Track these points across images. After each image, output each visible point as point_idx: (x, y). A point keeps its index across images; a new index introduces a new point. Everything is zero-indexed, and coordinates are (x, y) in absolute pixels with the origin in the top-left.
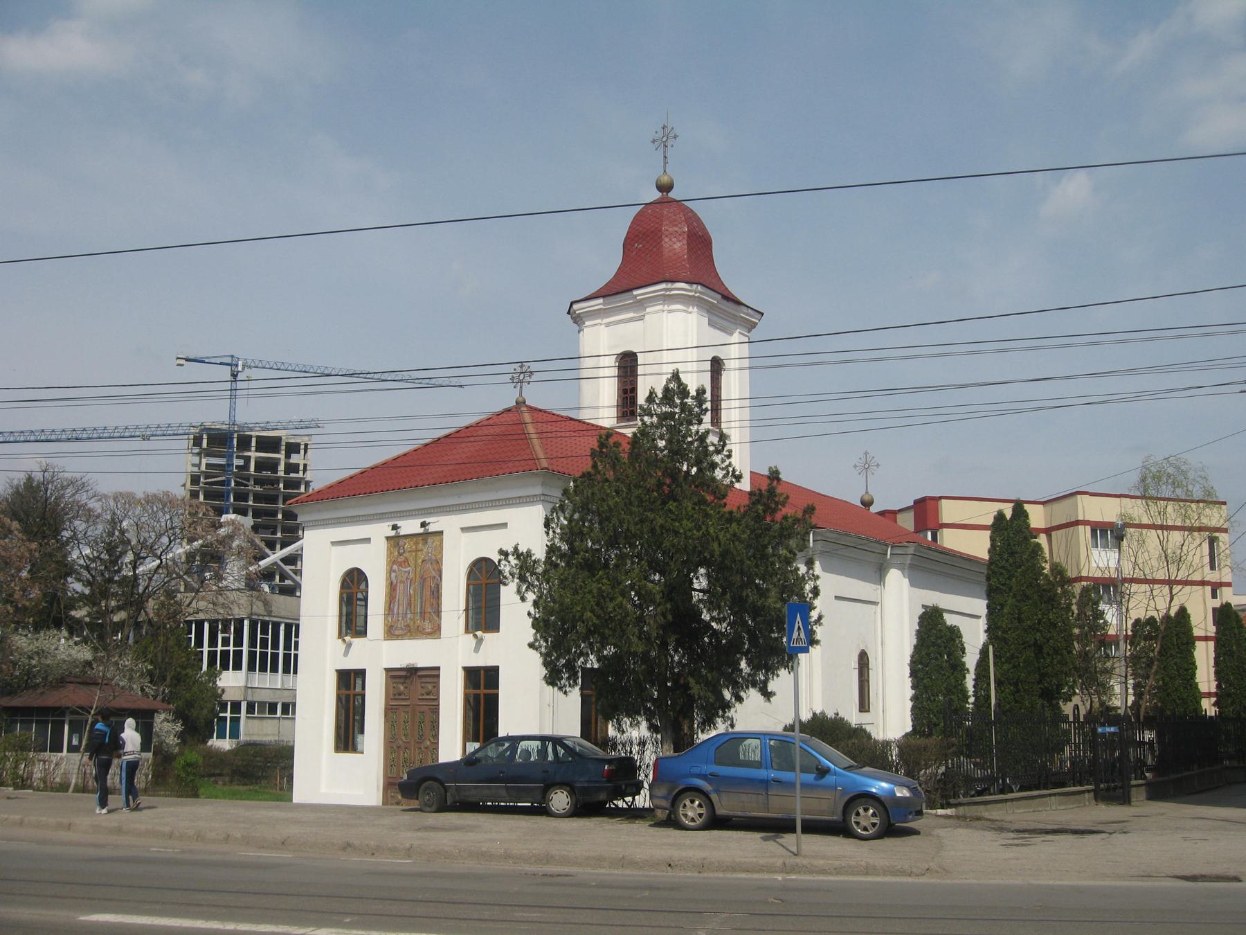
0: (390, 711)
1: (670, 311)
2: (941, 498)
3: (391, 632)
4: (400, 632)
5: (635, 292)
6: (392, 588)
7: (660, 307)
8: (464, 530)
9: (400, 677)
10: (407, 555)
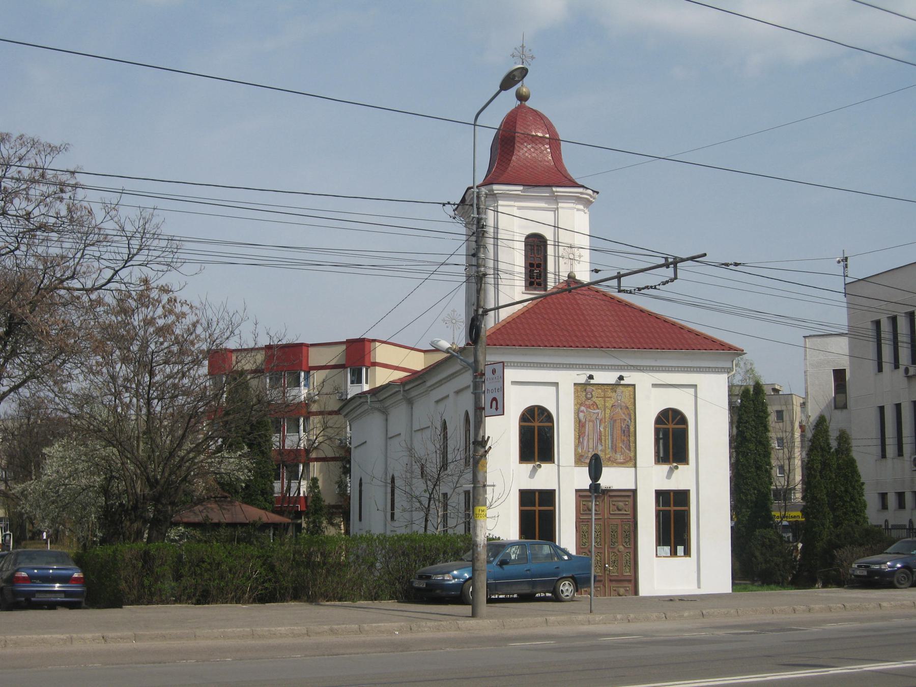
1: (578, 210)
2: (374, 341)
5: (554, 189)
6: (580, 426)
7: (571, 205)
8: (654, 385)
10: (594, 399)
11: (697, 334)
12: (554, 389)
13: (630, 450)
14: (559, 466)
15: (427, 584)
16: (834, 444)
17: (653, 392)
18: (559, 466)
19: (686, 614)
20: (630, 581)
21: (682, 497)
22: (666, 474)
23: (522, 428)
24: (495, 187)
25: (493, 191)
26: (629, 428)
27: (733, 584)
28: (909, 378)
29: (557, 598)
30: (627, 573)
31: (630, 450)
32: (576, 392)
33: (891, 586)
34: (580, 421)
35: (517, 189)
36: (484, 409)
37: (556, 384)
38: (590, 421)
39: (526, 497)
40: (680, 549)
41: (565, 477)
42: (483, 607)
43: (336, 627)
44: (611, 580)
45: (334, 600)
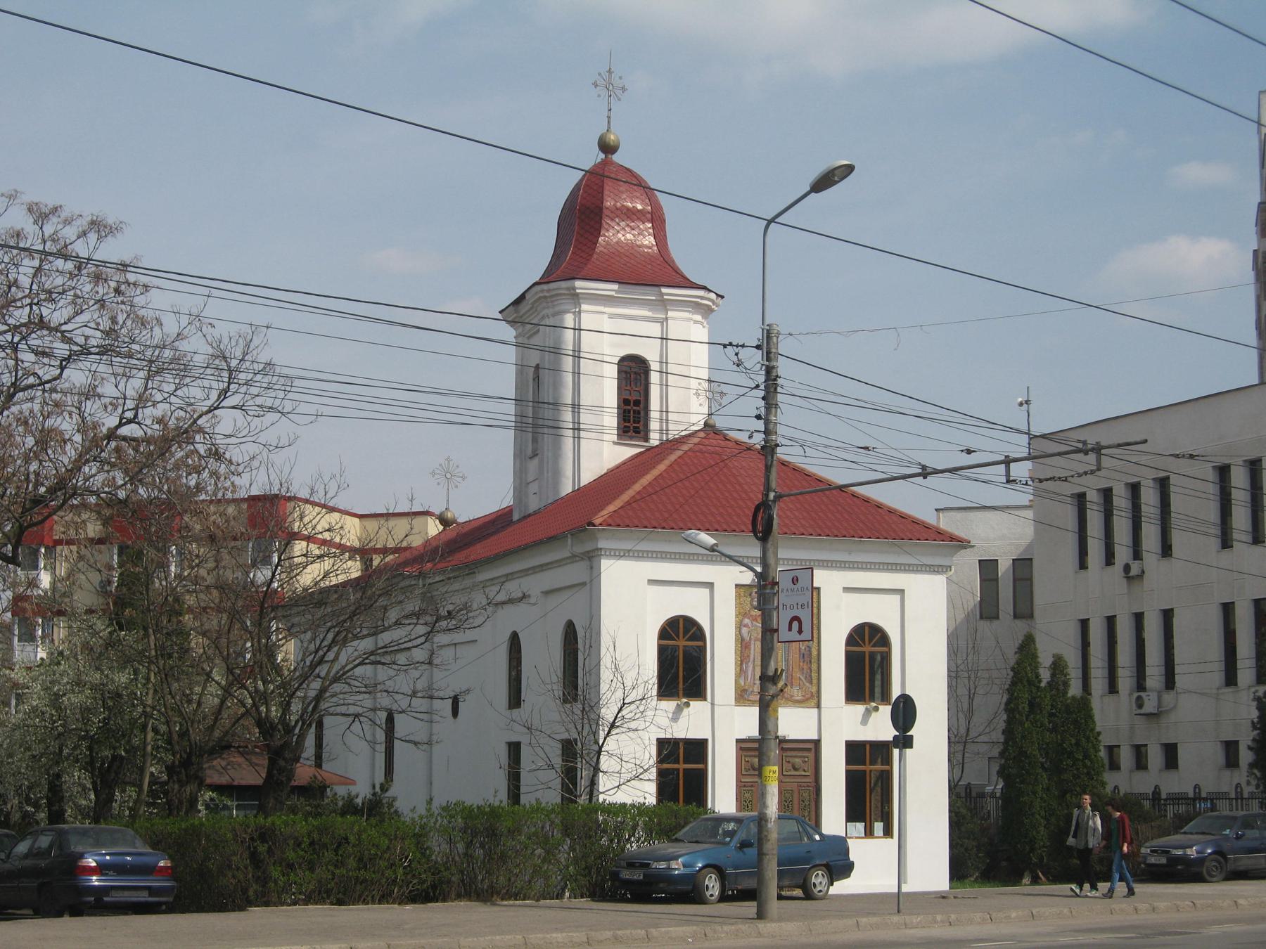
1: (696, 322)
5: (664, 290)
8: (846, 590)
11: (903, 517)
12: (705, 592)
14: (713, 704)
15: (645, 875)
16: (1045, 675)
17: (845, 598)
18: (713, 704)
19: (1014, 915)
23: (662, 651)
24: (578, 283)
25: (574, 289)
27: (951, 879)
28: (1129, 578)
29: (809, 896)
32: (738, 596)
33: (1198, 878)
34: (743, 639)
35: (610, 288)
36: (777, 630)
37: (710, 585)
40: (879, 827)
41: (722, 720)
42: (774, 906)
43: (619, 933)
45: (509, 899)
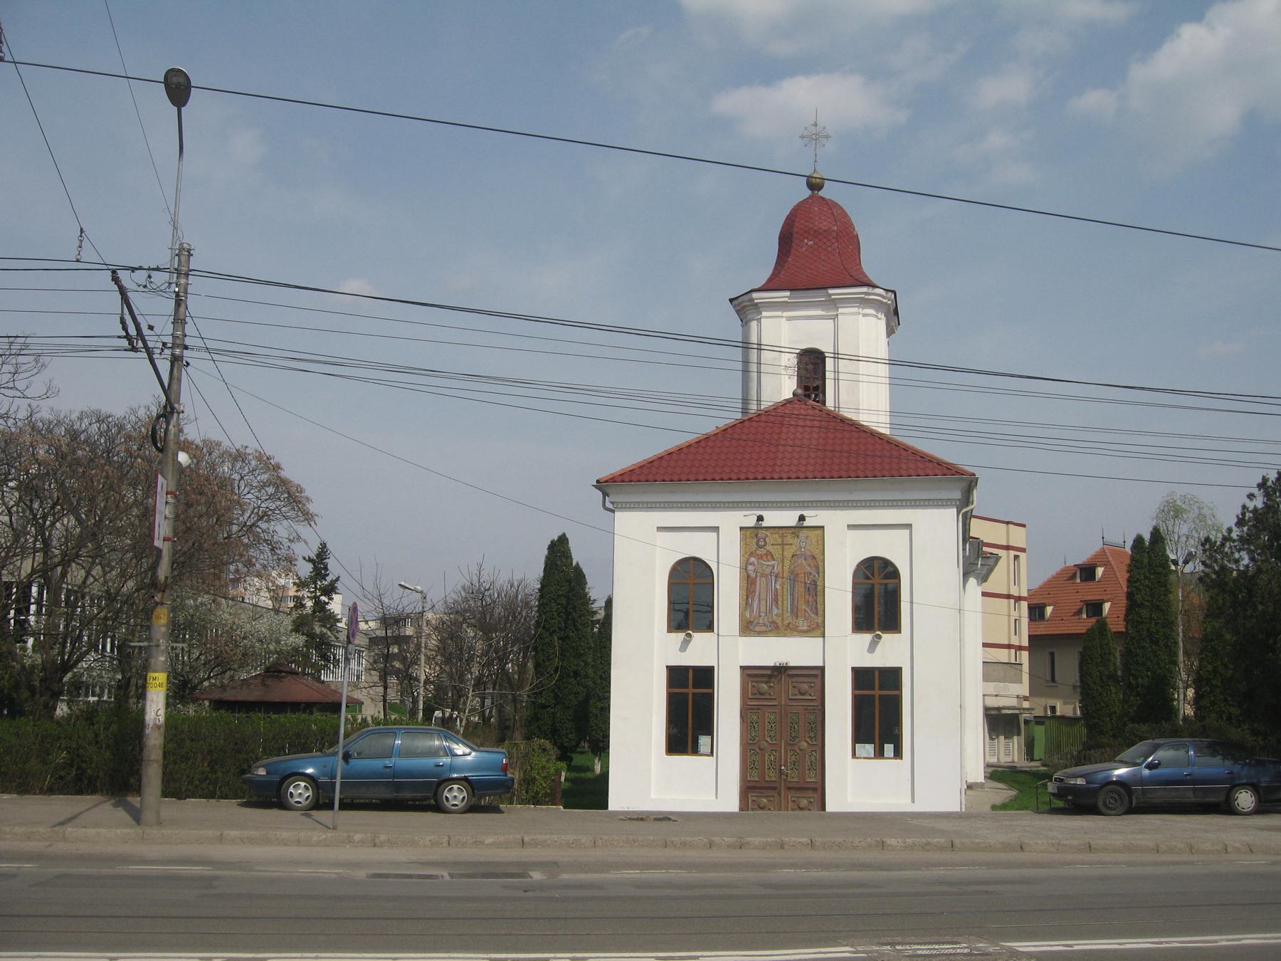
0: (747, 712)
1: (865, 315)
3: (748, 627)
4: (764, 628)
5: (831, 291)
6: (749, 585)
9: (763, 675)
10: (769, 547)
13: (817, 614)
17: (847, 538)
19: (489, 840)
20: (815, 790)
21: (891, 677)
22: (867, 645)
26: (816, 585)
30: (811, 778)
31: (817, 614)
32: (744, 540)
34: (748, 576)
38: (763, 575)
39: (676, 675)
40: (889, 749)
41: (729, 651)
44: (789, 788)
